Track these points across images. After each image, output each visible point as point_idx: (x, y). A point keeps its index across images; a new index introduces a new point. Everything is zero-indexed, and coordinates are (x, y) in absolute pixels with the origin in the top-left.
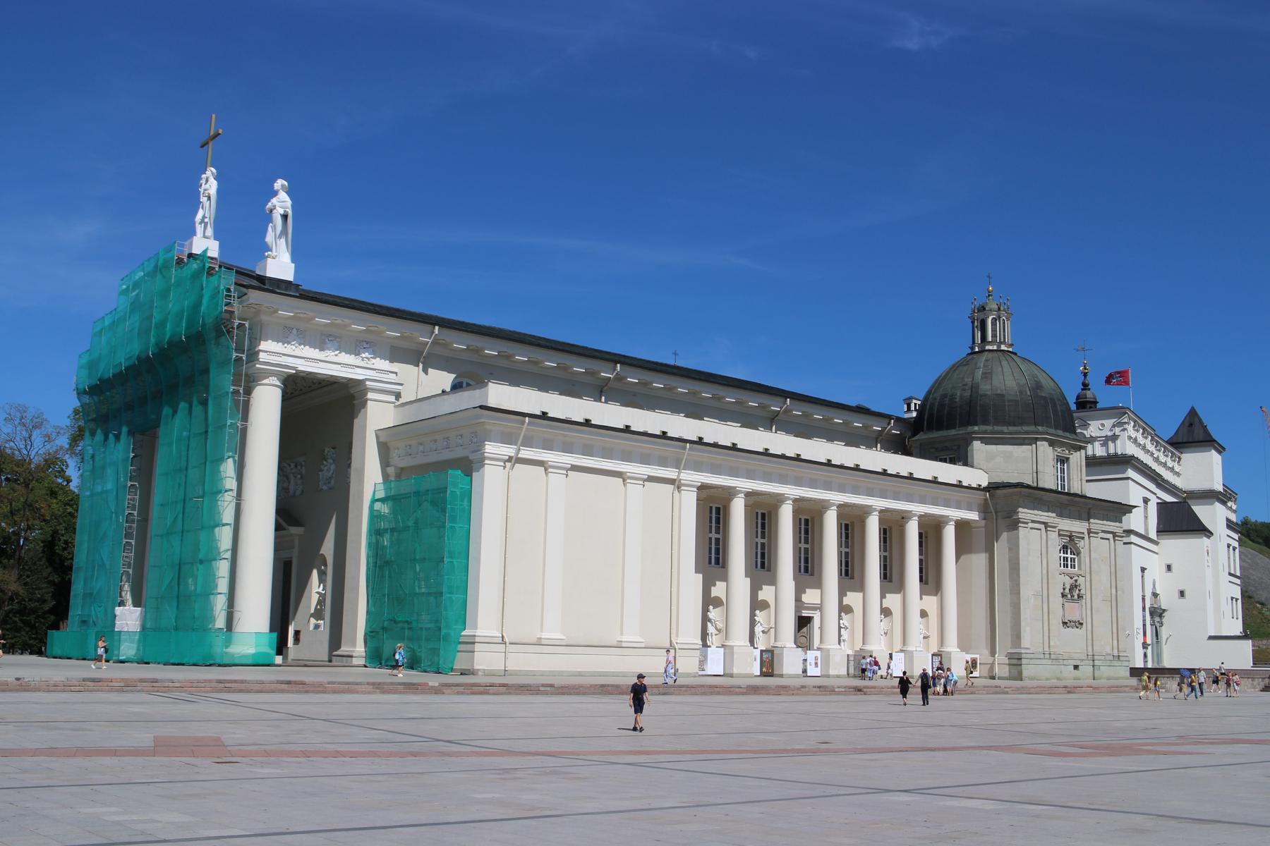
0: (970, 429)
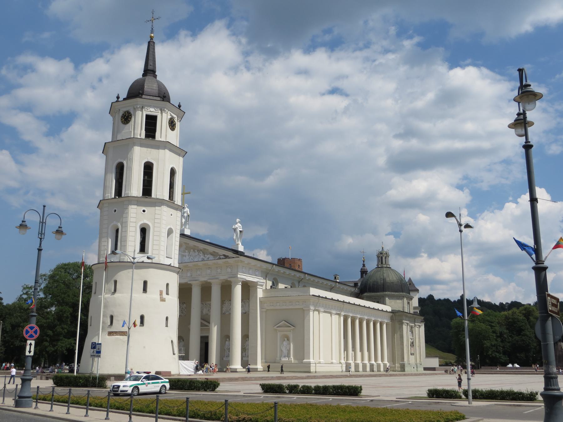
0: (384, 293)
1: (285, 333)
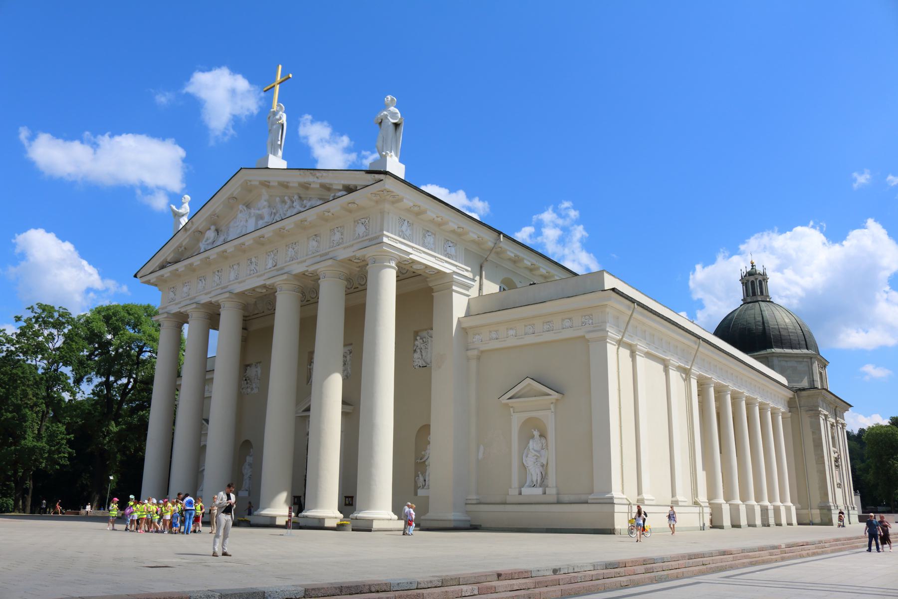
0: (769, 351)
1: (533, 414)
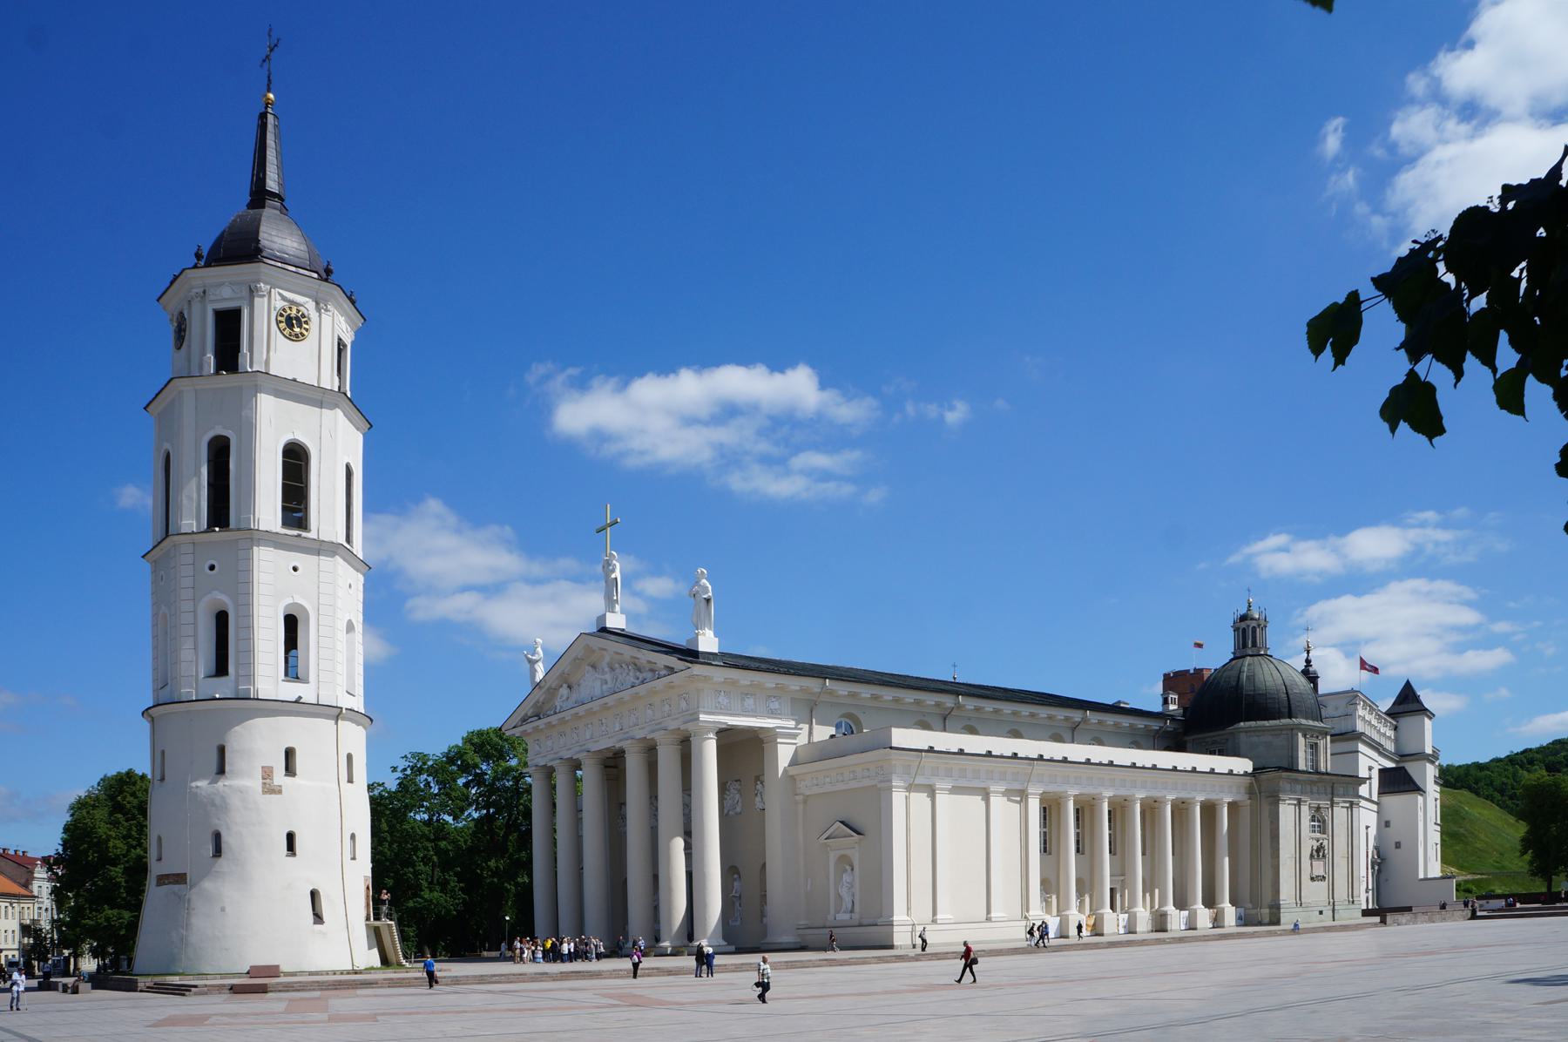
0: (1236, 726)
